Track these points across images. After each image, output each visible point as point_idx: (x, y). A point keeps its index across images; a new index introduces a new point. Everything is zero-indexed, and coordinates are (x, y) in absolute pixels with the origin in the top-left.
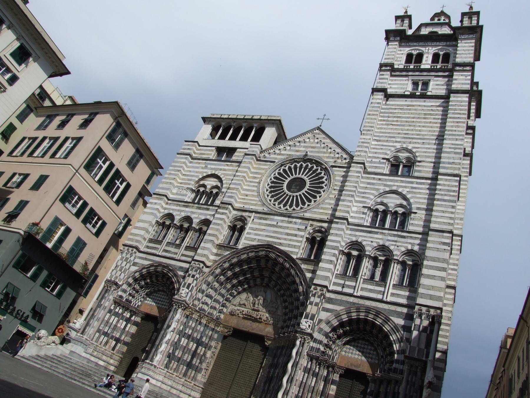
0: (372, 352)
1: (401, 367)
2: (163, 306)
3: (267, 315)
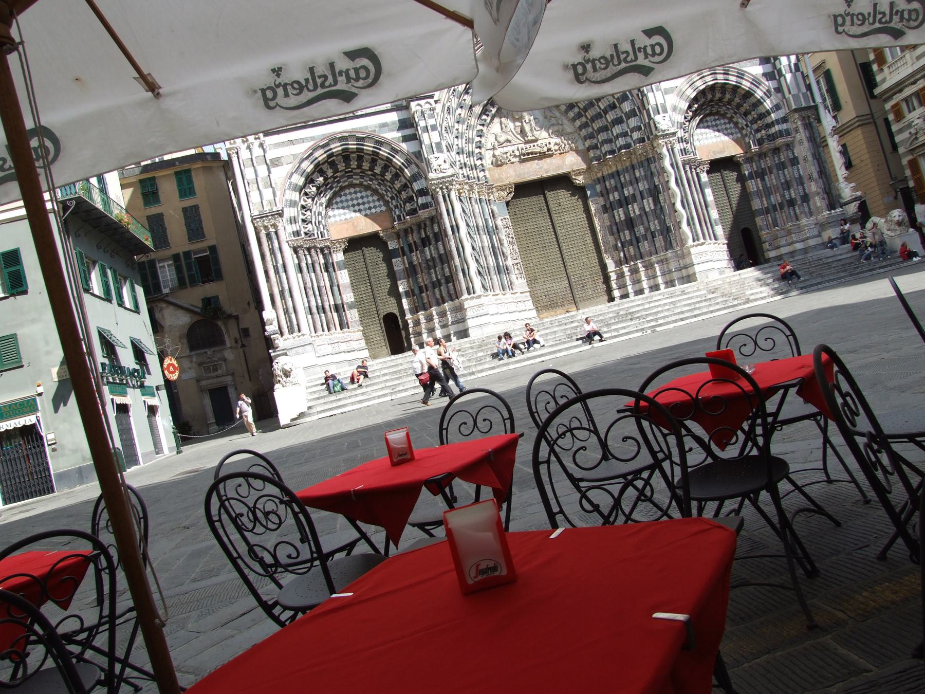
0: (728, 126)
1: (784, 126)
2: (373, 211)
3: (558, 140)
